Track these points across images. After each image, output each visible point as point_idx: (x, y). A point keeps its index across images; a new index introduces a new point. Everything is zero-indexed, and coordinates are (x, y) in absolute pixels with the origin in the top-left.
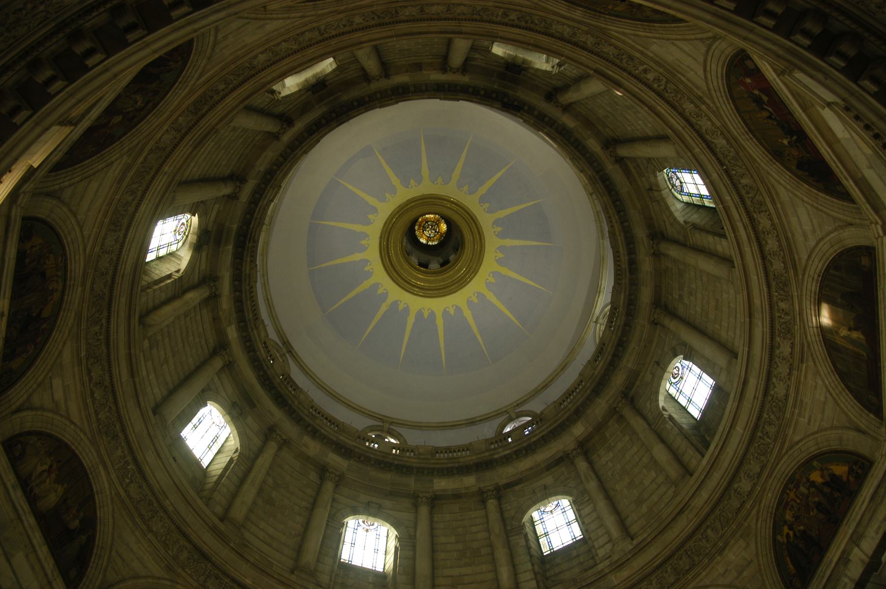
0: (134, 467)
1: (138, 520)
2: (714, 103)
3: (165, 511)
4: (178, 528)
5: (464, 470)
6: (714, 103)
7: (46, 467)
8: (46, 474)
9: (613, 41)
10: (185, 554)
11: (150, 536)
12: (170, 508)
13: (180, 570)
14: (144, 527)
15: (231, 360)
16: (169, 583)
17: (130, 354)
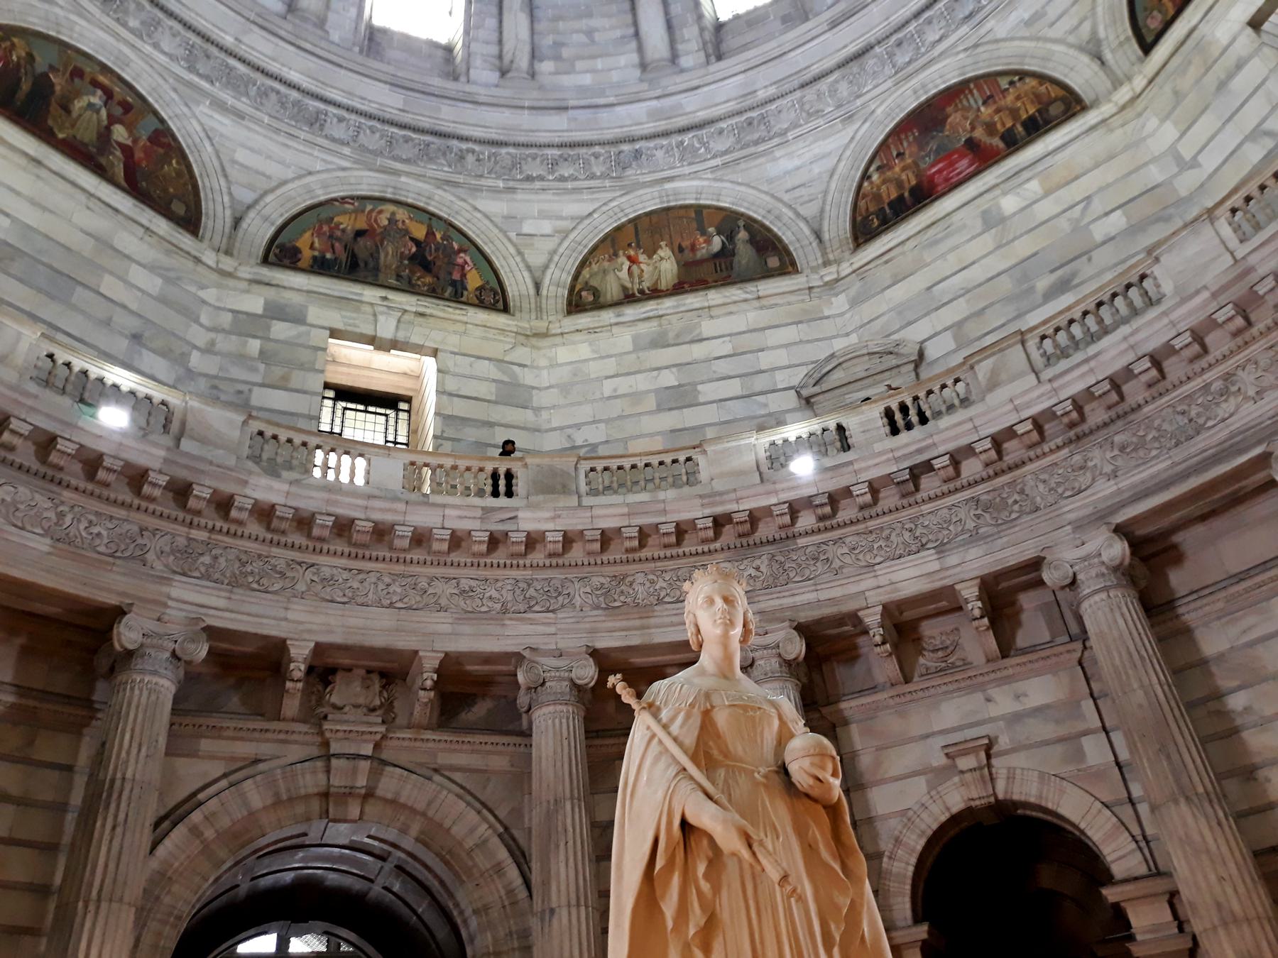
0: (690, 135)
1: (761, 148)
3: (771, 100)
4: (802, 86)
7: (627, 263)
8: (635, 267)
11: (790, 136)
12: (772, 91)
13: (859, 102)
14: (776, 141)
17: (532, 108)
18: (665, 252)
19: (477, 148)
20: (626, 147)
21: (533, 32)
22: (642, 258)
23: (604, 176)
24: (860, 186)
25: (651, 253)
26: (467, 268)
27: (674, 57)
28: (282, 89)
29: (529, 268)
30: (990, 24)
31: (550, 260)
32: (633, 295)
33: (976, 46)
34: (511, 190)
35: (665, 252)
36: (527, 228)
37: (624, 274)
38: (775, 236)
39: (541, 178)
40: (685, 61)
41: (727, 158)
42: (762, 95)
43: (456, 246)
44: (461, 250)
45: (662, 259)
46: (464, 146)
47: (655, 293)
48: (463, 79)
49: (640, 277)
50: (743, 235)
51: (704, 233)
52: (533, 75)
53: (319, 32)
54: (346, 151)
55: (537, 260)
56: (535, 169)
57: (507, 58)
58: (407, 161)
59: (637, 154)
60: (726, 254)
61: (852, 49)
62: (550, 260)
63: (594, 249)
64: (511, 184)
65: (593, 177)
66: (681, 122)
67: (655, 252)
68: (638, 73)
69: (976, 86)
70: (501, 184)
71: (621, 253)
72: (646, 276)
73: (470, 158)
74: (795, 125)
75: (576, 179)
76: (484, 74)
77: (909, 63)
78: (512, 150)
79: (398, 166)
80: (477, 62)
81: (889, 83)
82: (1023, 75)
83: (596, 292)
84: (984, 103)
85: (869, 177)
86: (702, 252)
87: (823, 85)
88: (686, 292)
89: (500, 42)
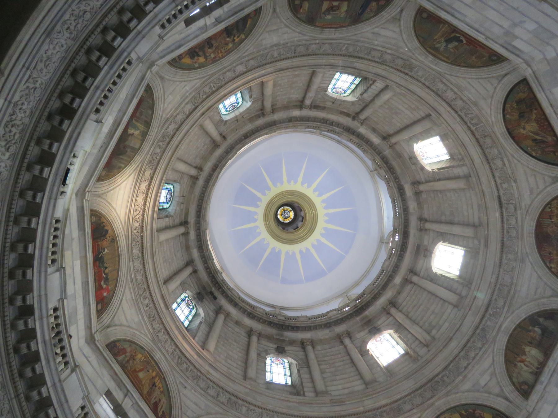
1: (512, 292)
2: (127, 277)
3: (497, 278)
4: (500, 266)
5: (359, 136)
6: (127, 277)
7: (522, 364)
8: (526, 363)
9: (152, 331)
10: (510, 256)
11: (515, 281)
12: (494, 277)
13: (519, 255)
14: (513, 286)
15: (408, 273)
16: (530, 257)
17: (444, 348)
18: (527, 349)
19: (444, 373)
20: (478, 331)
21: (421, 327)
22: (524, 357)
23: (483, 345)
24: (552, 272)
25: (524, 353)
26: (482, 415)
27: (460, 295)
28: (385, 409)
29: (498, 396)
30: (523, 204)
31: (500, 387)
32: (537, 372)
33: (527, 211)
34: (465, 377)
35: (527, 349)
36: (483, 382)
37: (525, 368)
38: (550, 310)
39: (469, 364)
40: (464, 293)
41: (507, 304)
42: (493, 280)
43: (471, 411)
44: (474, 411)
45: (529, 352)
46: (440, 376)
47: (542, 365)
48: (419, 358)
49: (531, 364)
50: (541, 320)
51: (530, 331)
52: (433, 338)
53: (377, 383)
54: (415, 411)
55: (497, 390)
56: (464, 363)
57: (423, 341)
58: (432, 397)
59: (483, 330)
60: (544, 330)
61: (499, 246)
62: (500, 387)
63: (507, 370)
64: (463, 374)
65: (481, 349)
66: (483, 310)
67: (525, 352)
68: (456, 309)
69: (542, 218)
70: (461, 378)
71: (516, 363)
72: (532, 362)
73: (445, 378)
74: (512, 278)
75: (477, 354)
76: (422, 351)
77: (517, 232)
78: (452, 365)
79: (431, 401)
80: (417, 349)
81: (520, 242)
82: (550, 203)
83: (525, 383)
84: (551, 219)
85: (551, 267)
86: (538, 338)
87: (505, 261)
88: (550, 354)
89: (417, 339)
